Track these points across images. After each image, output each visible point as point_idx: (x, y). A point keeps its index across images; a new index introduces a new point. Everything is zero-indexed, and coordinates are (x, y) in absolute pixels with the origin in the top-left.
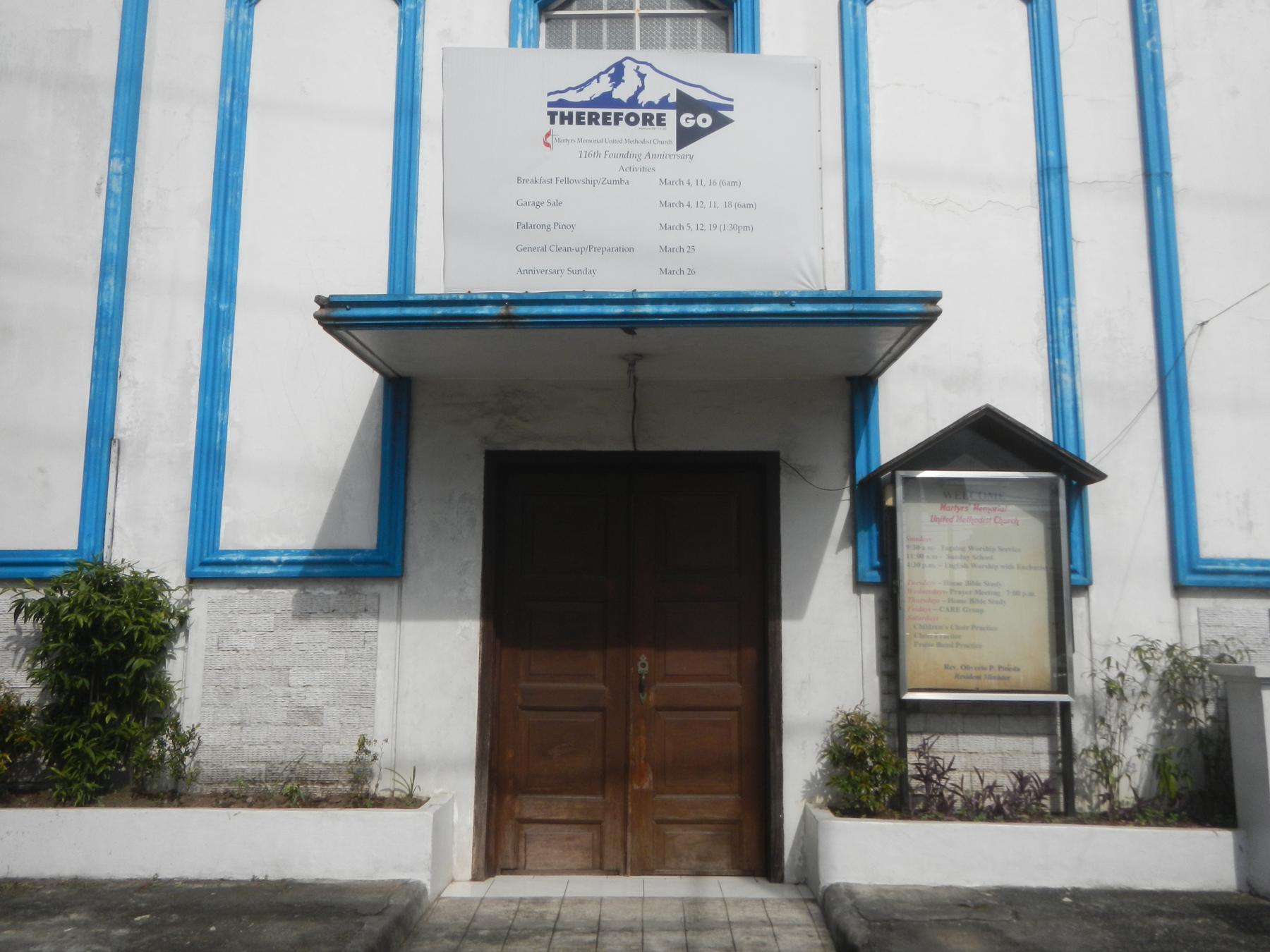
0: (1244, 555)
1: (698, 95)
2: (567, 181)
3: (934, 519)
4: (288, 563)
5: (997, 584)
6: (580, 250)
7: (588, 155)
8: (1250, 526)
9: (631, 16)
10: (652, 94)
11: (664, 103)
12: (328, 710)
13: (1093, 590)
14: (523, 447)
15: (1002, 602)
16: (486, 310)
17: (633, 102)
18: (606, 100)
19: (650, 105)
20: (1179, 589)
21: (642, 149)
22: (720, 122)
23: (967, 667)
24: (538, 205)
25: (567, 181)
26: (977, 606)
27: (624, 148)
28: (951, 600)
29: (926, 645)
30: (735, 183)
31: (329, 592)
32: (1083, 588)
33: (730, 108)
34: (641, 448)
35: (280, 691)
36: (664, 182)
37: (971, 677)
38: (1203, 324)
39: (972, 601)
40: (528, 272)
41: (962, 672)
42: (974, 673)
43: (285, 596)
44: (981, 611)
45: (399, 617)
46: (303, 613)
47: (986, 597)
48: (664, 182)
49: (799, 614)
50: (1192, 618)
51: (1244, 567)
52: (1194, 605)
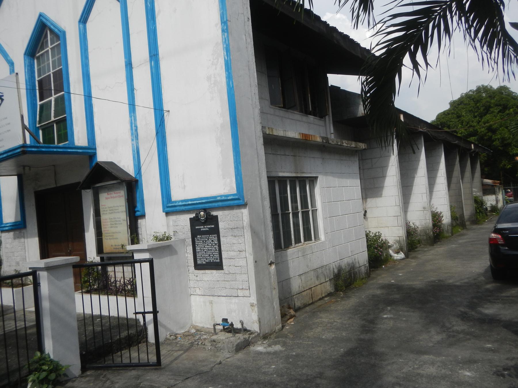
0: (183, 199)
3: (107, 198)
4: (10, 226)
5: (120, 218)
8: (185, 187)
9: (48, 51)
12: (21, 263)
13: (146, 217)
14: (40, 189)
15: (121, 224)
20: (168, 214)
23: (116, 245)
26: (116, 225)
28: (111, 224)
29: (107, 239)
30: (6, 118)
31: (17, 232)
32: (143, 216)
33: (3, 96)
34: (58, 185)
35: (13, 258)
37: (117, 249)
38: (169, 111)
39: (115, 224)
41: (115, 247)
42: (117, 247)
43: (11, 234)
44: (117, 227)
45: (27, 238)
46: (15, 238)
47: (117, 222)
49: (88, 231)
50: (171, 223)
51: (180, 204)
52: (173, 218)
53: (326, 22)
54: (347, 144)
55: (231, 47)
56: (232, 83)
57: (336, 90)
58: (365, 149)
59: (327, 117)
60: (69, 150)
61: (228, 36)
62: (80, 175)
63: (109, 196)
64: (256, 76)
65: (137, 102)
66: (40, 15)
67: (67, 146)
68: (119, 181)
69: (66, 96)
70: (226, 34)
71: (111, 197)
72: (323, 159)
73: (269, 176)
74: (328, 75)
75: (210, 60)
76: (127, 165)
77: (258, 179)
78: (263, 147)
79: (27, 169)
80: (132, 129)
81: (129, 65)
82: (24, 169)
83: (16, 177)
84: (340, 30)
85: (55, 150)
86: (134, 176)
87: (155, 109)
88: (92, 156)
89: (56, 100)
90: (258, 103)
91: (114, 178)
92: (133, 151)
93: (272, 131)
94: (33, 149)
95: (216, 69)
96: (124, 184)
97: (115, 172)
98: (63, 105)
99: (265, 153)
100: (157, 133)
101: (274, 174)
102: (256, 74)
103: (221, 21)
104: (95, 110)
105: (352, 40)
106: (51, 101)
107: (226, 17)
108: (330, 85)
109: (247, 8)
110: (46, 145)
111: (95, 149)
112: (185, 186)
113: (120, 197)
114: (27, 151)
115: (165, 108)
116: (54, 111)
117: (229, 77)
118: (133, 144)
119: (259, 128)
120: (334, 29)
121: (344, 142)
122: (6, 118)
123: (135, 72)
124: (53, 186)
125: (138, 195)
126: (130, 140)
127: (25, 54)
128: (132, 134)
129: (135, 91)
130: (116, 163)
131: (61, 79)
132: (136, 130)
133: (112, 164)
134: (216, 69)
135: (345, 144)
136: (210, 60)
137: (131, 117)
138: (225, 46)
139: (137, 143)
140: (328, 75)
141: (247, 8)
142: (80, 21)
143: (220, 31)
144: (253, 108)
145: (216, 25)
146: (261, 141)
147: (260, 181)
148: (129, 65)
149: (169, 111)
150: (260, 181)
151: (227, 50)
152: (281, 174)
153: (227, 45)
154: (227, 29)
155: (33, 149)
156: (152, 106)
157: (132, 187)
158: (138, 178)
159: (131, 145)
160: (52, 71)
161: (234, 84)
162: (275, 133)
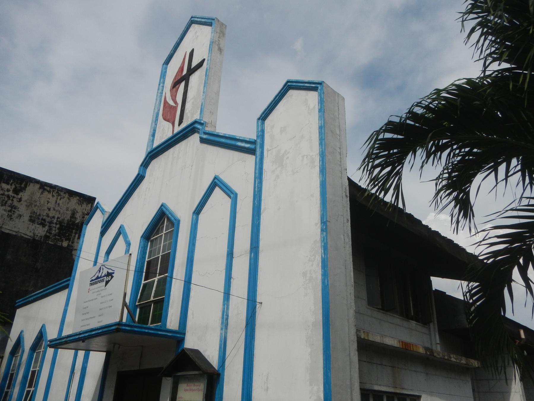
1: (110, 271)
2: (89, 301)
3: (185, 390)
6: (89, 319)
7: (94, 292)
8: (267, 389)
10: (103, 275)
11: (105, 276)
14: (123, 370)
16: (63, 340)
17: (101, 277)
18: (98, 278)
19: (103, 277)
21: (99, 289)
22: (112, 277)
24: (85, 308)
25: (89, 301)
27: (96, 290)
30: (111, 294)
33: (114, 273)
36: (102, 297)
38: (261, 303)
40: (82, 326)
48: (102, 297)
53: (427, 226)
54: (456, 359)
55: (328, 246)
56: (328, 281)
57: (441, 294)
58: (478, 367)
59: (431, 325)
60: (160, 333)
61: (326, 236)
62: (164, 361)
63: (188, 388)
64: (352, 276)
65: (233, 291)
66: (162, 205)
67: (157, 328)
68: (201, 372)
69: (168, 279)
70: (325, 233)
71: (190, 390)
72: (427, 374)
73: (362, 387)
74: (432, 278)
75: (307, 257)
76: (212, 356)
77: (349, 390)
78: (357, 353)
79: (117, 346)
80: (223, 318)
81: (230, 255)
82: (114, 346)
83: (105, 353)
84: (443, 234)
85: (147, 331)
86: (216, 368)
87: (248, 300)
88: (181, 341)
89: (159, 280)
90: (353, 304)
91: (196, 367)
92: (221, 341)
93: (368, 335)
94: (127, 328)
95: (312, 265)
96: (205, 375)
97: (198, 362)
98: (164, 287)
99: (359, 360)
100: (247, 325)
101: (368, 387)
102: (352, 273)
103: (321, 221)
104: (192, 294)
105: (457, 245)
106: (154, 281)
107: (326, 218)
108: (434, 289)
109: (347, 210)
110: (140, 325)
111: (185, 334)
112: (268, 388)
113: (199, 390)
114: (121, 329)
115: (258, 300)
116: (155, 291)
117: (325, 275)
118: (221, 334)
119: (353, 331)
120: (437, 233)
121: (452, 356)
122: (111, 294)
123: (235, 261)
124: (137, 368)
125: (217, 392)
126: (219, 329)
127: (142, 237)
128: (222, 323)
129: (232, 280)
130: (202, 351)
131: (167, 262)
132: (227, 319)
133: (197, 352)
134: (312, 265)
135: (453, 359)
136: (307, 257)
137: (224, 305)
138: (323, 244)
139: (226, 333)
140: (432, 278)
141: (347, 210)
142: (194, 213)
143: (319, 230)
144: (348, 309)
145: (316, 224)
146: (355, 346)
147: (351, 394)
148: (230, 255)
149: (261, 303)
150: (351, 394)
151: (325, 248)
152: (376, 388)
153: (324, 244)
154: (326, 228)
155: (127, 328)
156: (246, 296)
157: (213, 379)
158: (220, 372)
159: (219, 334)
160: (161, 254)
161: (329, 282)
162: (371, 339)
